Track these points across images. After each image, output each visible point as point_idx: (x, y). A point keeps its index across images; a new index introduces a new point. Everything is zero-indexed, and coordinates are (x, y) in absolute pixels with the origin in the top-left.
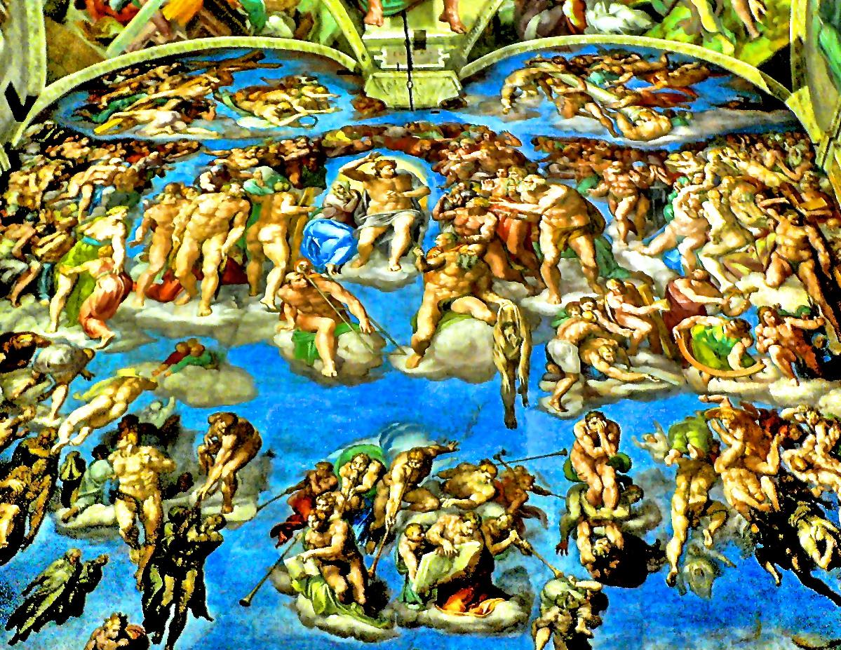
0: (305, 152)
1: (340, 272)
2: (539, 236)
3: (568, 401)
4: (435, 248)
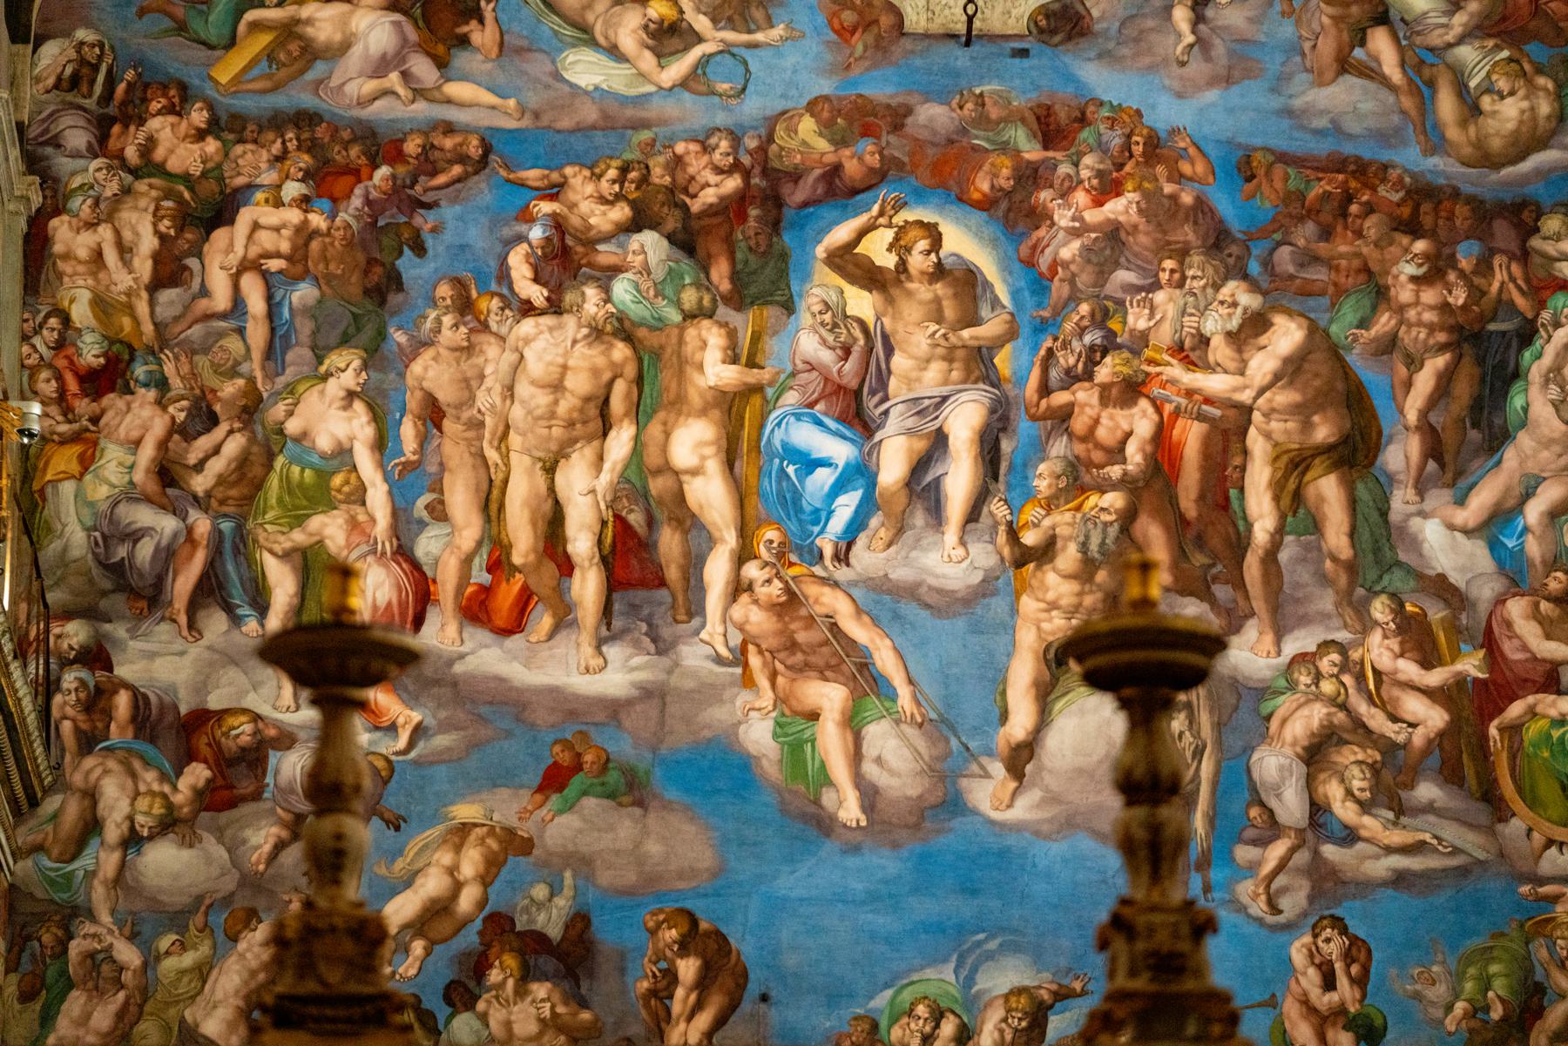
0: (733, 183)
1: (848, 565)
2: (1243, 469)
3: (1284, 890)
4: (1029, 496)
